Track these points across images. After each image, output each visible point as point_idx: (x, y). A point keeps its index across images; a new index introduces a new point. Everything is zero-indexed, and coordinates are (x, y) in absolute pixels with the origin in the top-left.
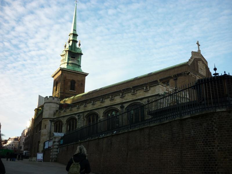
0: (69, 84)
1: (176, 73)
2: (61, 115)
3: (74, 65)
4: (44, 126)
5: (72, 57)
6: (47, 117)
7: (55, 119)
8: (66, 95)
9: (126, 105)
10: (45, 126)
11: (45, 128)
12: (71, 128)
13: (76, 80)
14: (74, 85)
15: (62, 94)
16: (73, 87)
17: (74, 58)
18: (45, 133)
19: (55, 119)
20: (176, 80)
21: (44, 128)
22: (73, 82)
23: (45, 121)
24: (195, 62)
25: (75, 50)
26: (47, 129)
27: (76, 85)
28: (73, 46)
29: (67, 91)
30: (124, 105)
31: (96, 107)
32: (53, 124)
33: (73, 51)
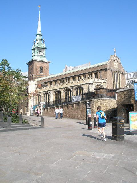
0: (39, 69)
1: (101, 69)
3: (41, 57)
5: (39, 51)
9: (74, 88)
12: (46, 98)
13: (43, 66)
14: (42, 70)
15: (35, 76)
16: (41, 71)
17: (41, 51)
20: (100, 73)
22: (41, 68)
24: (112, 62)
25: (41, 46)
27: (43, 70)
28: (40, 43)
29: (38, 74)
30: (74, 87)
31: (59, 88)
33: (40, 47)
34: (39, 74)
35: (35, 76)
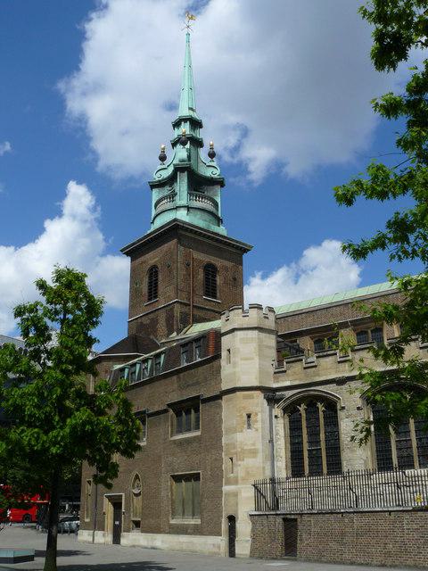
0: (201, 276)
2: (318, 375)
4: (246, 418)
6: (256, 383)
7: (288, 393)
8: (197, 313)
10: (249, 416)
11: (249, 426)
16: (210, 289)
18: (254, 445)
19: (288, 393)
21: (246, 426)
23: (251, 397)
26: (260, 430)
27: (219, 280)
32: (277, 411)
34: (202, 299)
35: (185, 309)
